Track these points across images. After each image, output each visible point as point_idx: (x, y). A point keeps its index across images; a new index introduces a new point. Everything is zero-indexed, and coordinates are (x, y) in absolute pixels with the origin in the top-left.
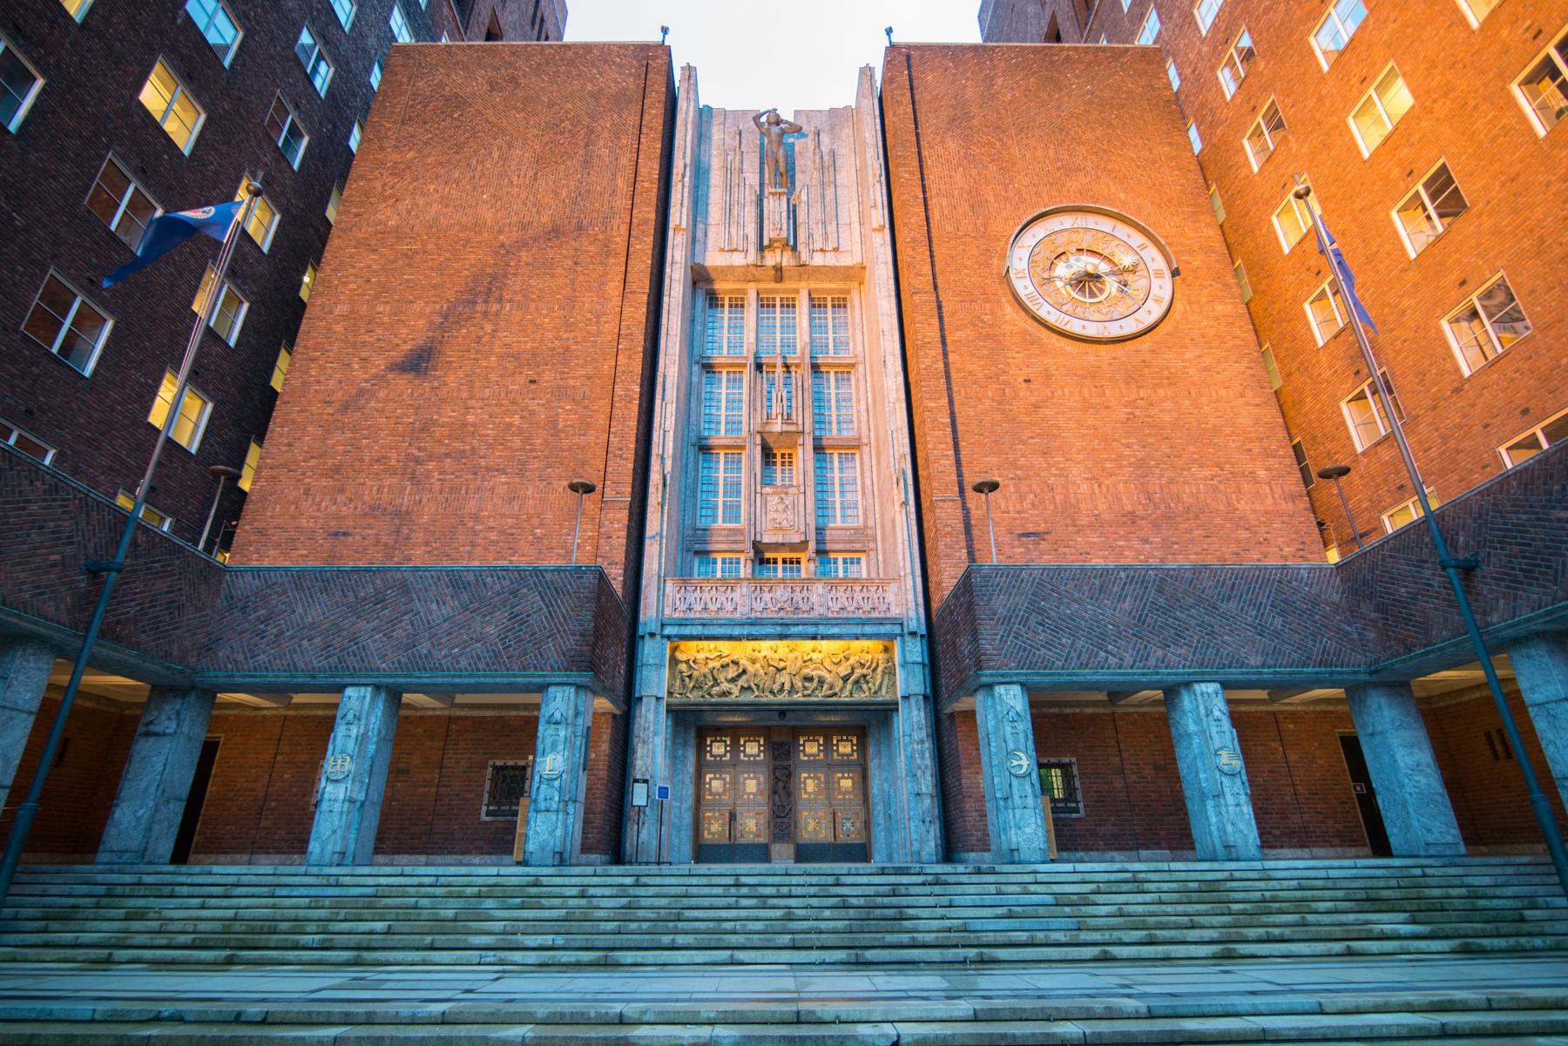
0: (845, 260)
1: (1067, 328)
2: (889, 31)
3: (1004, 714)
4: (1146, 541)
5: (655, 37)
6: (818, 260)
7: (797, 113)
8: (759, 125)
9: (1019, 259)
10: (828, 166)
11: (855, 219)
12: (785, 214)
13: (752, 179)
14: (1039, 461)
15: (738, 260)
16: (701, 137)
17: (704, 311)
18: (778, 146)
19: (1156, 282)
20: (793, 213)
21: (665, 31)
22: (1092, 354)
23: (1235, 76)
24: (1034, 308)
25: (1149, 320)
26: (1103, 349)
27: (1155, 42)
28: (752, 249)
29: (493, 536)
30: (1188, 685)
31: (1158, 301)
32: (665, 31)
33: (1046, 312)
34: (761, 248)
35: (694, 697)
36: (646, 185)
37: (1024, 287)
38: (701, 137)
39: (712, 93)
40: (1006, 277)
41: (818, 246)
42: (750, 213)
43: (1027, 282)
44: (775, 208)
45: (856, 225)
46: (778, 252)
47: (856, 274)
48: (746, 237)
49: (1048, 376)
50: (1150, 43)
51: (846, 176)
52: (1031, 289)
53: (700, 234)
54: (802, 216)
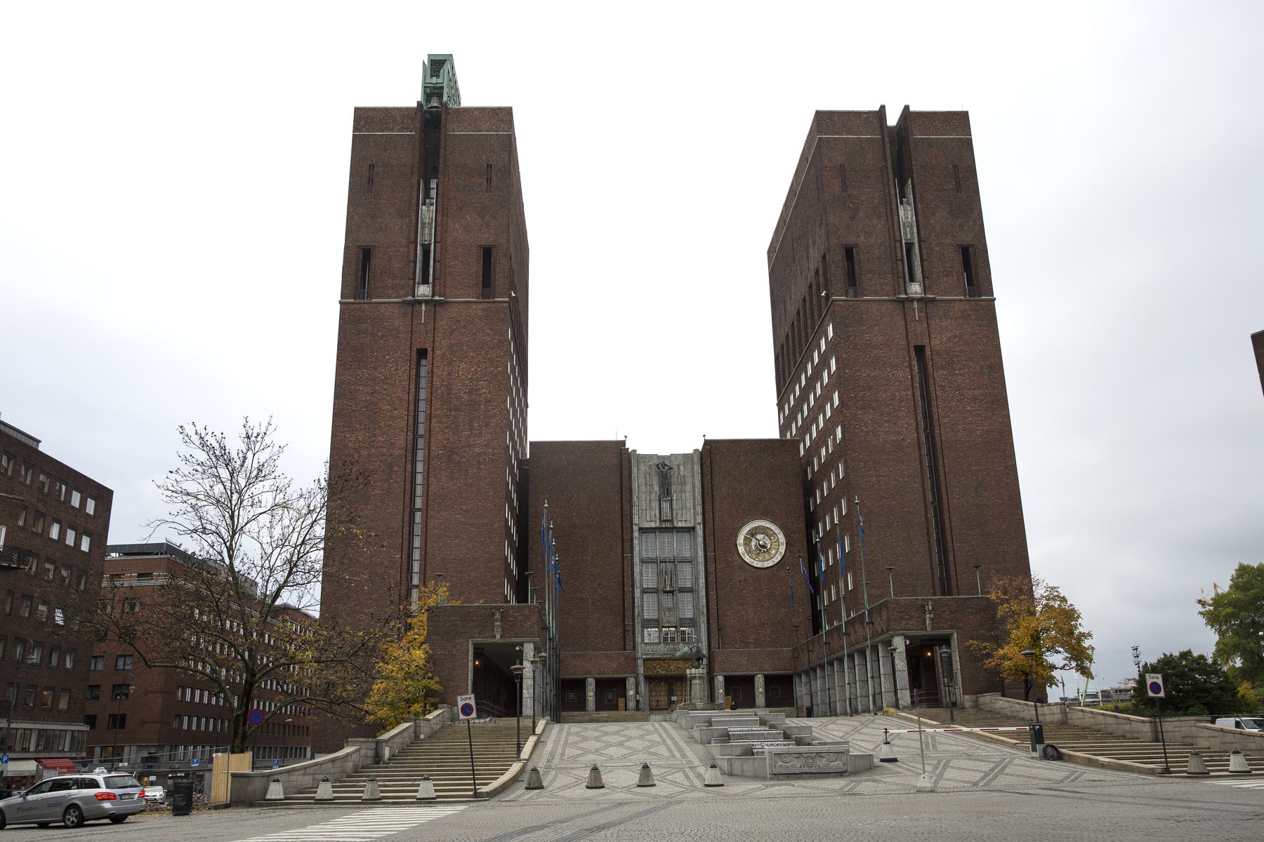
3: (720, 679)
5: (621, 438)
6: (680, 525)
9: (741, 540)
13: (656, 488)
15: (653, 525)
18: (664, 469)
20: (671, 506)
37: (741, 549)
42: (655, 504)
44: (665, 506)
47: (693, 528)
51: (688, 488)
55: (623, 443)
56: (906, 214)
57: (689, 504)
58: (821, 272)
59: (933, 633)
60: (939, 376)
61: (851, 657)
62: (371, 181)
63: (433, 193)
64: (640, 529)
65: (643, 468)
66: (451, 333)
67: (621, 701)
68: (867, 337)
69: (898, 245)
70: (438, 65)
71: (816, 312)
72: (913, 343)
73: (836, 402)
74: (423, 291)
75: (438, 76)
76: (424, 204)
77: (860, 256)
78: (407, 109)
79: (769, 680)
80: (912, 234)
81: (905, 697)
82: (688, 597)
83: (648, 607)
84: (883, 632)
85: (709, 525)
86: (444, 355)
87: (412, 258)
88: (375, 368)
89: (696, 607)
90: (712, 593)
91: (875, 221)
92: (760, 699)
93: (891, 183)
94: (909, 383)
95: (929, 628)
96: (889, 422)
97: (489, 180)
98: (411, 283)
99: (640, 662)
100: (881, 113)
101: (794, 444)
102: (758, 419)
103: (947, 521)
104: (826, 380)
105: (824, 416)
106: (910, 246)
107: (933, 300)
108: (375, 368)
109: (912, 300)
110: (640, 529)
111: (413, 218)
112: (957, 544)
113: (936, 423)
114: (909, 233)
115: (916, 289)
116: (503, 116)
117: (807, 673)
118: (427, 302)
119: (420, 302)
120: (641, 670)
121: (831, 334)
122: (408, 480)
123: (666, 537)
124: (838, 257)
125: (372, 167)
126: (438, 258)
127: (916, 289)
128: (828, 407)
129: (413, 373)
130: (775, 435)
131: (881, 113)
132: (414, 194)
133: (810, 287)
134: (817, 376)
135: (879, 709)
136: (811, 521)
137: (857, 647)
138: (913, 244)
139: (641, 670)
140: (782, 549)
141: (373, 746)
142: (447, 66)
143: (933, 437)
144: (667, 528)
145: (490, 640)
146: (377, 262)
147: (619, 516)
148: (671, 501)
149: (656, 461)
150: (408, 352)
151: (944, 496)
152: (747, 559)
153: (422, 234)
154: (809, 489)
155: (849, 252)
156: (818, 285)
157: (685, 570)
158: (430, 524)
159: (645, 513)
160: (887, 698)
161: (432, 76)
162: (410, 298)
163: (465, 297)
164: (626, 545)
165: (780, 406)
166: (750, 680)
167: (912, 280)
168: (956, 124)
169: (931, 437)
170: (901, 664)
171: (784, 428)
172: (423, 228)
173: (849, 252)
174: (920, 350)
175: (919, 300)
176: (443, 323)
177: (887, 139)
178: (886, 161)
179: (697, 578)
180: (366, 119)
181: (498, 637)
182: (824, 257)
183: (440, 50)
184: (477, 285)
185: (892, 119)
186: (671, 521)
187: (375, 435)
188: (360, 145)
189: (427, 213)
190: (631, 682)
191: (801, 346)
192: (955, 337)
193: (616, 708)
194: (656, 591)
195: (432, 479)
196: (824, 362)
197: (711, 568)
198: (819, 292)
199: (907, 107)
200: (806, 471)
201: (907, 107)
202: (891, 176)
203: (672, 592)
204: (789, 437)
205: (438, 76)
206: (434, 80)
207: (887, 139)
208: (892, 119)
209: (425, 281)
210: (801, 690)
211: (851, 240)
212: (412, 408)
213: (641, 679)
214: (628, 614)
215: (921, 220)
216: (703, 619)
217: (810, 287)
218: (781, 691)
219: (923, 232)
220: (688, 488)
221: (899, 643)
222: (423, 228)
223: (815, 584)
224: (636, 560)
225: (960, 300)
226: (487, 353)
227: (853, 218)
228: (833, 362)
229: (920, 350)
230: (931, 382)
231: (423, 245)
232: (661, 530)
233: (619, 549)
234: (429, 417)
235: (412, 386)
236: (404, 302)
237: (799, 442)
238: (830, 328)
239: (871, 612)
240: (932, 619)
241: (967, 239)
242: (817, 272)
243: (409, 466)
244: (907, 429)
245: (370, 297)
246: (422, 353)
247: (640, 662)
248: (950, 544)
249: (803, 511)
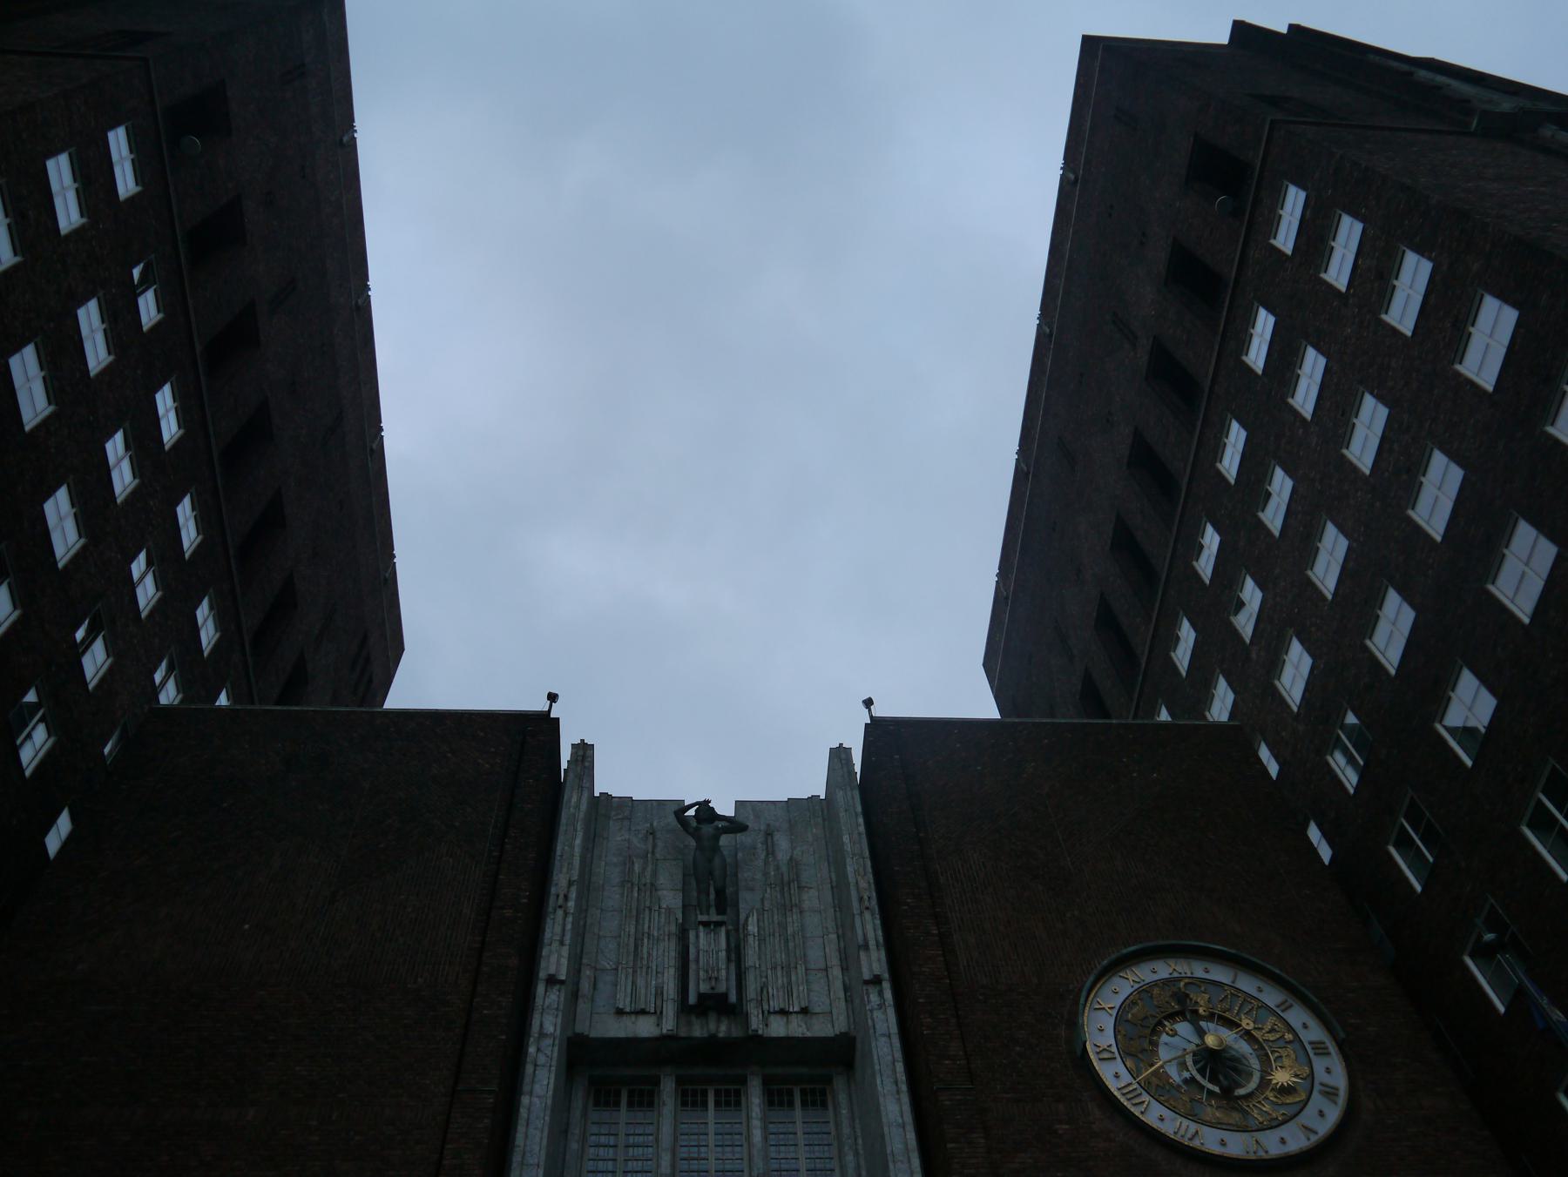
0: (820, 1028)
1: (1196, 1144)
2: (868, 703)
5: (541, 705)
6: (778, 1028)
7: (740, 805)
9: (1099, 1030)
10: (789, 883)
11: (834, 960)
12: (723, 954)
13: (671, 898)
15: (645, 1028)
16: (593, 838)
17: (585, 1114)
19: (1319, 1064)
20: (736, 953)
21: (552, 697)
23: (1351, 760)
24: (1136, 1111)
25: (1324, 1127)
27: (1232, 715)
28: (670, 1010)
31: (1330, 1093)
32: (552, 697)
33: (1155, 1114)
34: (684, 1008)
36: (508, 913)
37: (1114, 1075)
38: (593, 838)
39: (609, 780)
41: (775, 1004)
42: (665, 955)
45: (836, 972)
46: (712, 1017)
47: (841, 1054)
48: (659, 992)
50: (1224, 718)
52: (1126, 1078)
53: (585, 986)
54: (751, 957)
57: (821, 949)
64: (581, 1054)
110: (581, 1054)
144: (715, 1058)
149: (675, 808)
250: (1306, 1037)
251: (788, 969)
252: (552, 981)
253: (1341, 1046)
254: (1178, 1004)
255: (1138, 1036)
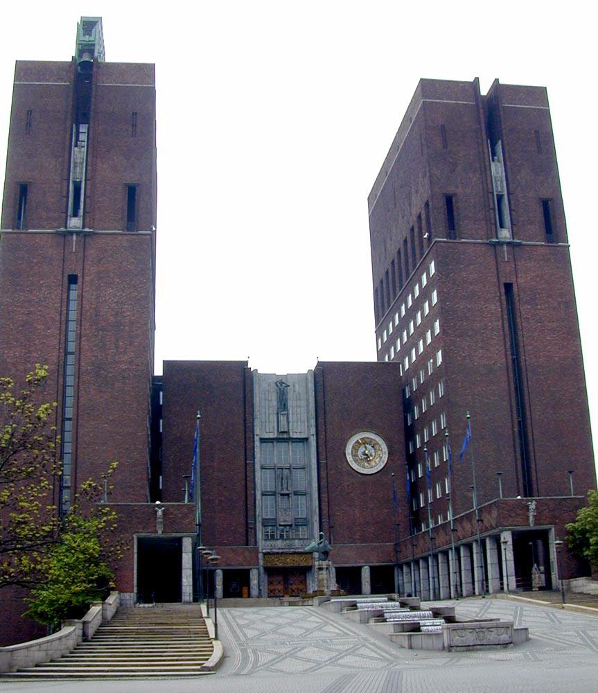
4: (370, 528)
8: (277, 386)
11: (306, 421)
13: (275, 403)
14: (348, 508)
15: (271, 436)
18: (282, 386)
22: (364, 478)
26: (368, 477)
28: (276, 432)
29: (222, 529)
30: (363, 566)
31: (383, 462)
34: (278, 430)
35: (269, 565)
37: (349, 458)
40: (345, 454)
43: (351, 456)
47: (307, 439)
49: (353, 484)
55: (246, 363)
56: (497, 170)
57: (304, 418)
58: (423, 217)
59: (538, 528)
60: (523, 309)
61: (458, 550)
62: (29, 124)
63: (83, 137)
64: (261, 439)
65: (265, 385)
66: (99, 261)
67: (245, 590)
68: (464, 275)
69: (490, 196)
70: (89, 26)
71: (417, 251)
72: (503, 280)
73: (437, 331)
74: (75, 223)
75: (90, 35)
76: (76, 146)
77: (458, 204)
78: (66, 62)
79: (373, 570)
80: (502, 187)
81: (513, 584)
82: (301, 500)
83: (264, 508)
84: (492, 528)
85: (322, 437)
86: (92, 280)
87: (65, 193)
88: (31, 291)
89: (310, 508)
90: (324, 496)
91: (471, 175)
92: (366, 586)
93: (485, 142)
94: (500, 315)
95: (532, 525)
96: (482, 348)
97: (134, 126)
98: (64, 215)
99: (260, 556)
100: (475, 84)
101: (394, 366)
102: (358, 343)
103: (530, 434)
104: (427, 311)
105: (425, 342)
106: (500, 198)
107: (520, 244)
108: (31, 291)
109: (501, 244)
110: (261, 439)
111: (66, 156)
112: (538, 454)
113: (521, 350)
114: (500, 187)
115: (505, 234)
116: (146, 72)
117: (408, 564)
118: (78, 233)
119: (71, 233)
120: (261, 562)
121: (433, 270)
122: (60, 392)
123: (284, 445)
124: (441, 203)
125: (30, 113)
126: (88, 194)
127: (505, 234)
128: (429, 334)
129: (65, 296)
130: (373, 358)
131: (475, 84)
132: (68, 136)
133: (412, 229)
134: (418, 304)
135: (485, 591)
136: (409, 433)
137: (464, 541)
138: (502, 195)
139: (261, 562)
140: (385, 458)
141: (81, 626)
142: (97, 27)
143: (519, 363)
144: (284, 438)
145: (153, 535)
146: (32, 196)
147: (242, 428)
148: (288, 415)
150: (60, 277)
151: (528, 413)
152: (355, 466)
153: (74, 173)
154: (408, 406)
155: (449, 201)
156: (420, 228)
157: (299, 475)
158: (81, 432)
159: (265, 426)
160: (493, 584)
161: (84, 35)
162: (63, 229)
163: (112, 229)
164: (249, 454)
165: (379, 333)
166: (359, 569)
167: (502, 226)
168: (538, 95)
169: (516, 361)
170: (508, 555)
171: (380, 354)
172: (75, 167)
173: (449, 201)
174: (508, 287)
175: (508, 244)
176: (91, 253)
177: (481, 106)
178: (480, 124)
179: (310, 483)
180: (27, 72)
181: (160, 532)
182: (427, 204)
183: (91, 13)
184: (122, 219)
185: (484, 90)
186: (287, 432)
187: (30, 352)
188: (20, 93)
189: (79, 154)
190: (254, 575)
191: (401, 280)
192: (538, 276)
193: (240, 596)
194: (274, 494)
195: (82, 392)
196: (425, 294)
197: (323, 474)
198: (421, 235)
199: (497, 80)
200: (404, 391)
201: (497, 80)
202: (485, 137)
203: (288, 495)
204: (387, 360)
205: (90, 35)
206: (87, 38)
207: (481, 106)
208: (484, 90)
209: (75, 214)
210: (404, 579)
211: (451, 190)
212: (63, 327)
213: (262, 570)
214: (250, 513)
215: (509, 177)
216: (316, 518)
217: (412, 229)
218: (384, 583)
219: (511, 185)
220: (303, 403)
221: (507, 537)
222: (75, 167)
223: (415, 489)
224: (258, 467)
225: (542, 246)
226: (131, 280)
227: (453, 171)
228: (435, 294)
229: (508, 287)
230: (518, 314)
231: (75, 182)
232: (278, 440)
233: (242, 457)
234: (80, 337)
235: (64, 308)
236: (57, 233)
237: (399, 364)
238: (433, 265)
239: (480, 511)
240: (534, 516)
241: (545, 193)
242: (419, 217)
243: (61, 380)
244: (498, 356)
245: (26, 227)
246: (73, 279)
247: (260, 556)
248: (532, 454)
249: (403, 425)
250: (383, 450)
251: (297, 422)
252: (257, 435)
253: (389, 453)
254: (365, 442)
255: (355, 448)
